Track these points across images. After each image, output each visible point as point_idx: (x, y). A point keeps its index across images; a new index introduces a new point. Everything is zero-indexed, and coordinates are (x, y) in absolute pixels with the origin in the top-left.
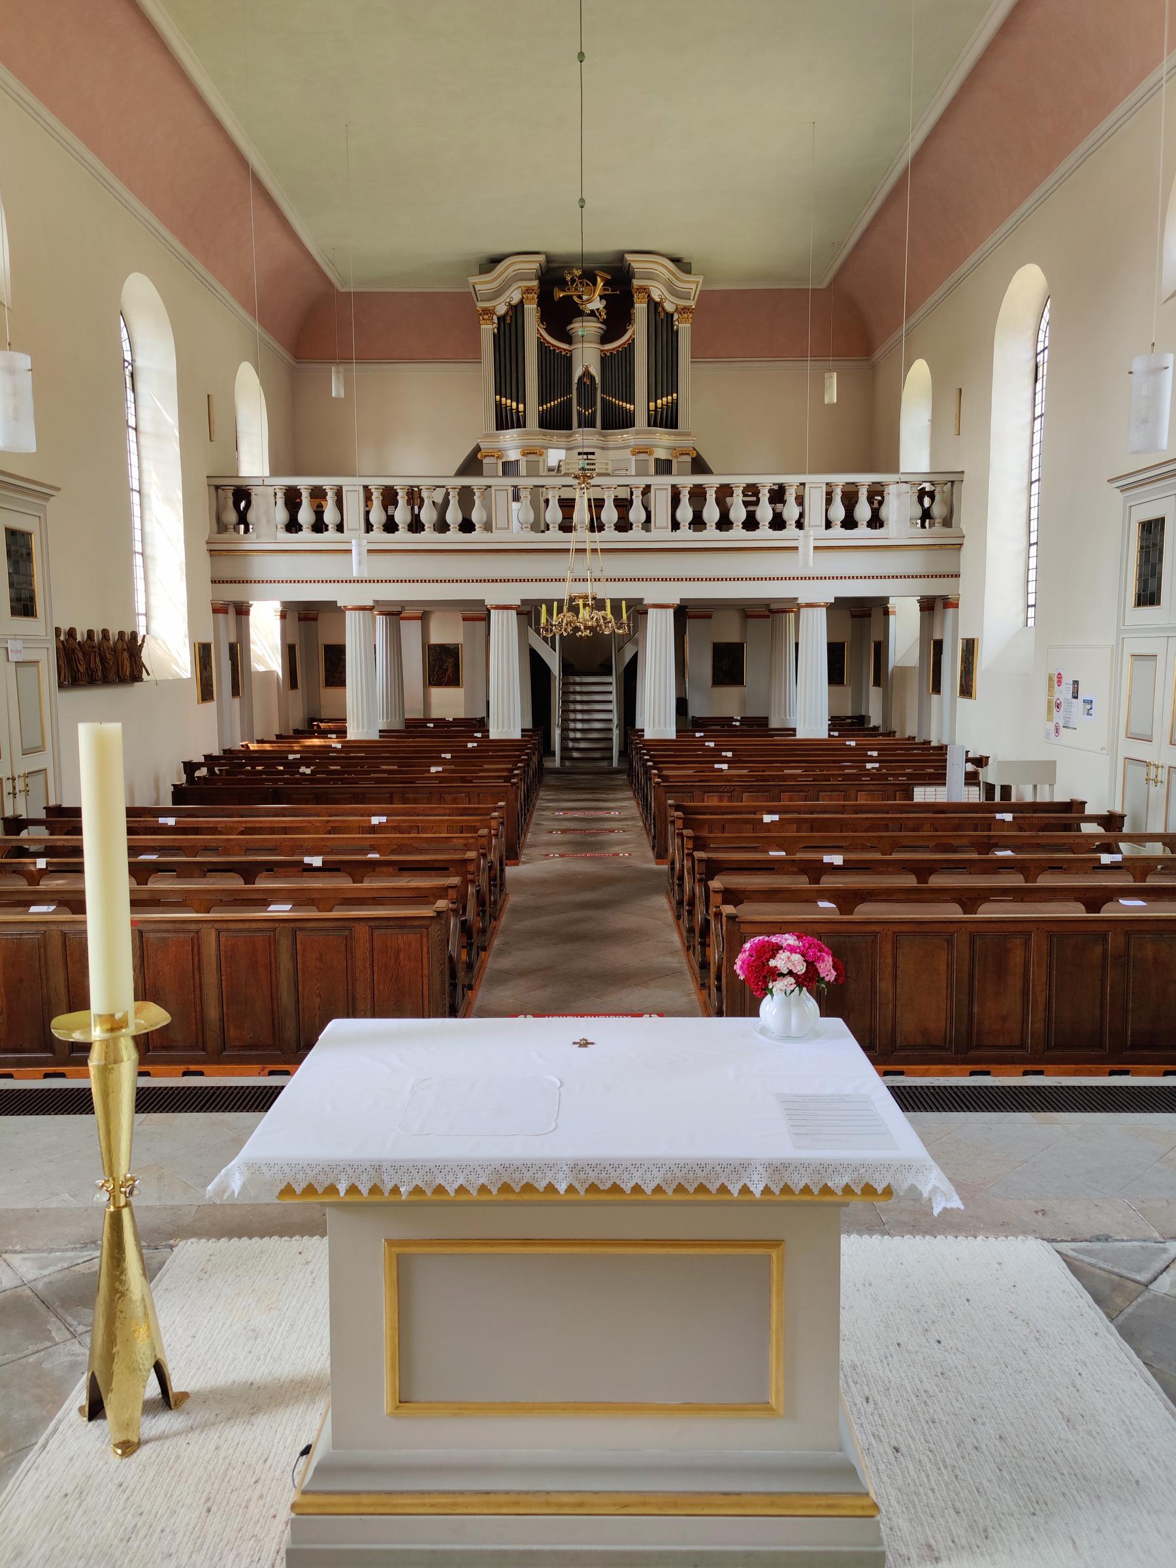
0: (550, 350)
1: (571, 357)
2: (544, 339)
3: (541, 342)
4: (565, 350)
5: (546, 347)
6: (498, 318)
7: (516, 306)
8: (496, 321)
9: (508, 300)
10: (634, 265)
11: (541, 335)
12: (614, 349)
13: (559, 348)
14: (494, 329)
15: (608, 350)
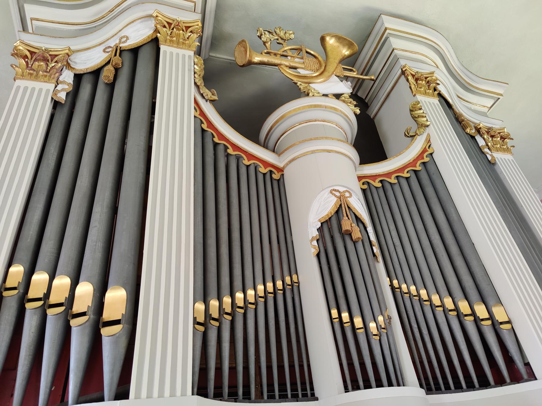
0: (228, 155)
1: (280, 182)
2: (210, 125)
3: (203, 131)
4: (266, 164)
5: (216, 145)
6: (78, 78)
7: (135, 51)
8: (68, 77)
9: (112, 43)
10: (395, 42)
11: (202, 114)
12: (389, 175)
13: (251, 156)
14: (55, 92)
15: (374, 177)
